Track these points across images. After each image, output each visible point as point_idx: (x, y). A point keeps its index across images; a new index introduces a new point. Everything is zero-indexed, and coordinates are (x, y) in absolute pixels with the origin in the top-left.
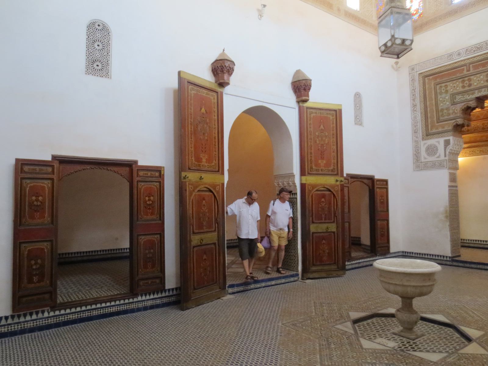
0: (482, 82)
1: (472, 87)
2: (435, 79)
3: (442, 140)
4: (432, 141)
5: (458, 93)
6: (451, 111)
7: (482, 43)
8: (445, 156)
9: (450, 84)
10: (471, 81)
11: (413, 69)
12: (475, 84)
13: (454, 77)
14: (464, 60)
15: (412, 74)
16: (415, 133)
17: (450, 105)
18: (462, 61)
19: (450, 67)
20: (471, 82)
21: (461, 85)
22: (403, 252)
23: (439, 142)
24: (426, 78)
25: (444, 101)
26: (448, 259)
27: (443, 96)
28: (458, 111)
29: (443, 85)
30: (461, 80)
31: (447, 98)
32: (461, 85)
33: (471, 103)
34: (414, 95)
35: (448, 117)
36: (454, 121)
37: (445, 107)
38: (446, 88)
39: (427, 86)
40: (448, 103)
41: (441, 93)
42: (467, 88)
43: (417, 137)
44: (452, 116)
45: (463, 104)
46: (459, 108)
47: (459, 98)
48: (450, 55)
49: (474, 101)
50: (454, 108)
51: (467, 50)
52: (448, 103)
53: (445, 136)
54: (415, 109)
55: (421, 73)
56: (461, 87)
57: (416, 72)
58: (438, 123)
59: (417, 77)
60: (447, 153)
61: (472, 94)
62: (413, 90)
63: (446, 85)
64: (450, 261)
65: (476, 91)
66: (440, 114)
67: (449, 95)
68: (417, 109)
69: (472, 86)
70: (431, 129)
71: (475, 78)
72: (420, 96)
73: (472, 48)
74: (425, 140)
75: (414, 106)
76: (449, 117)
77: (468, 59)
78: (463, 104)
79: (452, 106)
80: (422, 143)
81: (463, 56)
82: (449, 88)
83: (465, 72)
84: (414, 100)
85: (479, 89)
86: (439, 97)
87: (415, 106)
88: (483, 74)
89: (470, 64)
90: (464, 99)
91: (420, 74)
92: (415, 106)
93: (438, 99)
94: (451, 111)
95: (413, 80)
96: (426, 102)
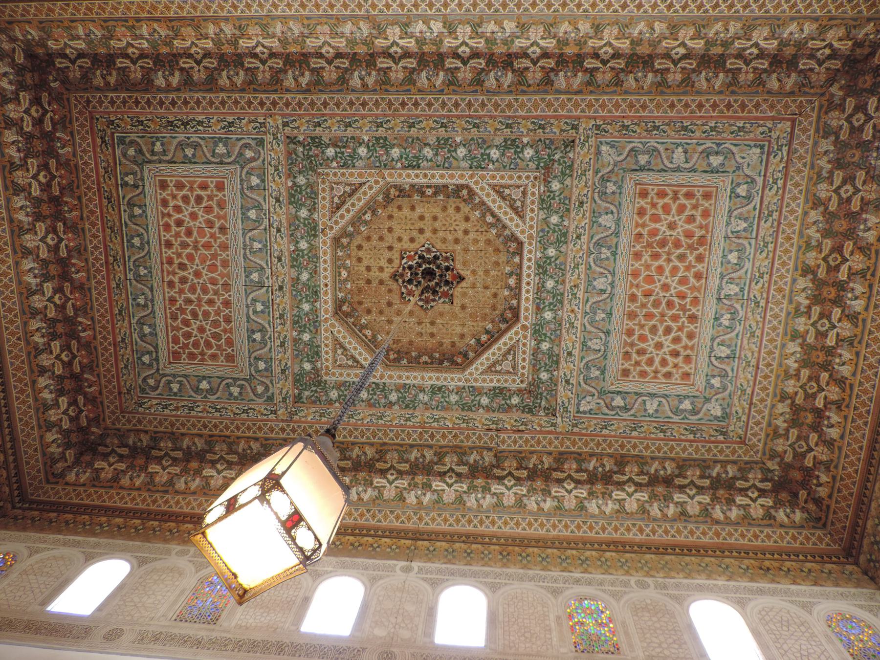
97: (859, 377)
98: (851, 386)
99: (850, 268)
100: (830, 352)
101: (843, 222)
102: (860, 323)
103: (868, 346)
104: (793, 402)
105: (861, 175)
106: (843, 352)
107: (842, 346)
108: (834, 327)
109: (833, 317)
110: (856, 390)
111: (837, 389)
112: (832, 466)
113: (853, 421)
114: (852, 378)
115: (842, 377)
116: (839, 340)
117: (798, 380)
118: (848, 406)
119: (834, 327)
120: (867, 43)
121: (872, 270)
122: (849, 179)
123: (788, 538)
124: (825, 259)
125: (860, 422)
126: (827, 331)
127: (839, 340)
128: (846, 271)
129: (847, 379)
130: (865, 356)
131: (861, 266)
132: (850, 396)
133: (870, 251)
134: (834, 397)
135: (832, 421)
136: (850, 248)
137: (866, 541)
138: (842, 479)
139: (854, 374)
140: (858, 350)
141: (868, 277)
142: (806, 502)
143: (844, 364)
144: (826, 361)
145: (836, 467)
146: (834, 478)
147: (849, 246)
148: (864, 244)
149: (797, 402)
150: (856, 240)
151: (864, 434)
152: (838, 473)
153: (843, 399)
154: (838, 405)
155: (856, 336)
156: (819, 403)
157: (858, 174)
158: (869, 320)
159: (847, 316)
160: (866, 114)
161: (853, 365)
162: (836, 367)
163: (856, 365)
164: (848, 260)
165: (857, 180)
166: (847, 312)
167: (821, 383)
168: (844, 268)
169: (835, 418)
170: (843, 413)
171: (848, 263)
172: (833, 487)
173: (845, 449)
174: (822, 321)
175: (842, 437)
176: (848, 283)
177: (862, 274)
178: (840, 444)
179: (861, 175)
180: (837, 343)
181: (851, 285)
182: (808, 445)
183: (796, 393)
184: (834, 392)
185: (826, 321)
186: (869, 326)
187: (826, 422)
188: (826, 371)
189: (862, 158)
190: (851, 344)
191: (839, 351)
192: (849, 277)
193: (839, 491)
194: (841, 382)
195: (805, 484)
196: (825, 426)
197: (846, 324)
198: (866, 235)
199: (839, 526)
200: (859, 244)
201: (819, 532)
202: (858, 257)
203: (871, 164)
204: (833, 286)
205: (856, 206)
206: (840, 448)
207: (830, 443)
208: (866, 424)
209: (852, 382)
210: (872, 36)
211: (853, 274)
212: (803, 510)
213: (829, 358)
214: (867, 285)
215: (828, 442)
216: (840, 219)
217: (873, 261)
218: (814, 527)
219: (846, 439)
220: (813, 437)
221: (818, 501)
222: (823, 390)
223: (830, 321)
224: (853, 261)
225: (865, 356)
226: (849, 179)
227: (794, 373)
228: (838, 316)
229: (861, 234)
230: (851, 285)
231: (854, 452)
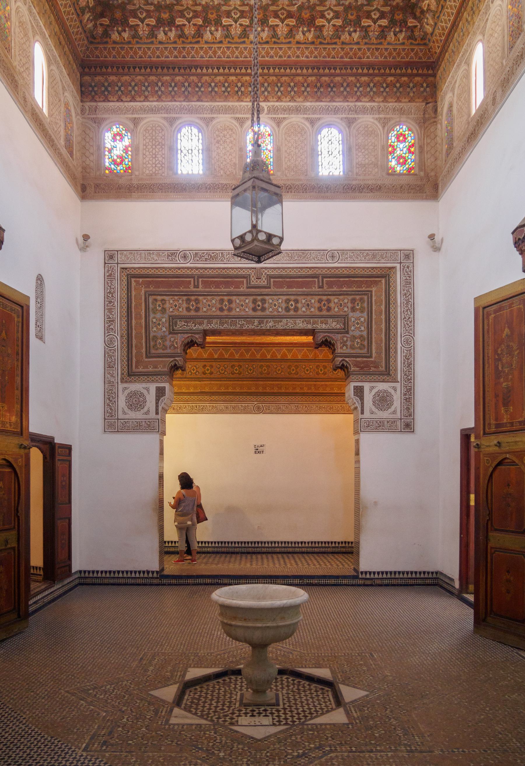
0: (214, 309)
1: (200, 313)
2: (148, 284)
3: (153, 387)
4: (136, 387)
5: (181, 318)
6: (168, 343)
7: (218, 252)
8: (157, 413)
9: (170, 301)
10: (199, 303)
11: (111, 257)
12: (205, 309)
13: (176, 289)
14: (192, 268)
15: (110, 265)
16: (110, 367)
17: (167, 333)
18: (188, 268)
19: (170, 272)
20: (200, 305)
21: (185, 305)
22: (80, 572)
23: (148, 390)
24: (133, 280)
25: (159, 324)
26: (155, 575)
27: (159, 315)
28: (179, 345)
29: (159, 298)
30: (185, 298)
31: (164, 320)
32: (185, 305)
33: (197, 336)
34: (110, 302)
35: (163, 352)
36: (172, 359)
37: (159, 334)
38: (163, 304)
39: (133, 293)
40: (164, 329)
41: (155, 311)
42: (193, 313)
43: (112, 376)
44: (169, 351)
45: (186, 336)
46: (180, 340)
47: (180, 325)
48: (172, 254)
49: (201, 335)
50: (172, 339)
51: (196, 253)
52: (164, 329)
53: (157, 381)
54: (112, 327)
55: (126, 269)
56: (185, 309)
57: (118, 263)
58: (147, 357)
59: (117, 275)
60: (160, 409)
61: (200, 324)
62: (110, 292)
63: (163, 300)
64: (157, 578)
65: (206, 321)
66: (152, 344)
67: (166, 316)
68: (114, 327)
69: (201, 311)
70: (137, 367)
71: (205, 301)
72: (121, 307)
73: (204, 253)
74: (126, 382)
75: (110, 321)
76: (165, 352)
77: (197, 268)
78: (186, 336)
79: (171, 335)
80: (121, 386)
81: (191, 262)
82: (167, 305)
83: (192, 288)
84: (110, 311)
85: (210, 318)
86: (152, 315)
87: (113, 321)
88: (216, 297)
89: (199, 277)
90: (187, 328)
91: (123, 268)
92: (113, 321)
93: (150, 319)
94: (168, 343)
95: (110, 275)
96: (131, 319)
97: (206, 46)
98: (198, 42)
99: (277, 26)
100: (218, 23)
101: (308, 15)
102: (242, 40)
103: (228, 48)
104: (175, 5)
105: (339, 22)
106: (220, 32)
107: (224, 30)
108: (236, 22)
109: (242, 20)
110: (196, 46)
111: (193, 32)
112: (137, 39)
113: (175, 48)
114: (204, 42)
115: (202, 34)
116: (227, 28)
117: (193, 5)
118: (183, 42)
119: (236, 22)
120: (422, 16)
121: (278, 41)
122: (337, 15)
123: (76, 30)
124: (283, 8)
125: (176, 53)
126: (232, 17)
127: (227, 28)
128: (275, 23)
129: (202, 38)
130: (221, 47)
131: (280, 33)
132: (191, 43)
133: (290, 38)
134: (186, 31)
135: (169, 33)
136: (291, 24)
137: (100, 78)
138: (131, 48)
139: (206, 42)
140: (224, 42)
141: (273, 40)
142: (101, 25)
143: (212, 34)
144: (211, 20)
145: (138, 43)
146: (129, 43)
147: (292, 22)
148: (294, 33)
149: (175, 7)
150: (297, 27)
151: (168, 57)
152: (134, 44)
153: (187, 38)
154: (182, 36)
155: (233, 38)
156: (179, 21)
157: (340, 20)
158: (245, 46)
159: (245, 30)
160: (378, 19)
161: (212, 41)
162: (208, 28)
163: (214, 43)
164: (283, 23)
165: (336, 20)
166: (247, 29)
167: (193, 20)
168: (277, 22)
169: (172, 35)
170: (178, 40)
171: (281, 24)
172: (122, 43)
173: (152, 46)
174: (238, 12)
175: (161, 43)
176: (267, 26)
177: (275, 35)
178: (155, 42)
179: (339, 22)
180: (225, 26)
181: (266, 29)
182: (145, 18)
183: (182, 5)
184: (190, 30)
185: (238, 15)
186: (241, 46)
187: (167, 29)
188: (203, 22)
189: (351, 21)
190: (226, 37)
191: (220, 29)
192: (271, 26)
193: (122, 48)
194: (199, 34)
195: (114, 22)
196: (164, 29)
197: (239, 30)
198: (300, 33)
199: (97, 53)
200: (294, 29)
201: (86, 42)
202: (286, 30)
203: (346, 28)
204: (264, 15)
205: (319, 22)
206: (152, 43)
207: (153, 35)
208: (176, 57)
209: (201, 42)
210: (426, 20)
211: (274, 29)
212: (95, 26)
213: (213, 23)
214: (269, 40)
215: (153, 33)
216: (310, 12)
217: (284, 41)
218: (87, 38)
219: (161, 46)
220: (152, 21)
221: (106, 34)
222: (189, 22)
223: (238, 18)
224: (283, 27)
225: (221, 47)
226: (337, 15)
227: (198, 3)
228: (244, 23)
229: (301, 29)
230: (266, 29)
231: (153, 53)
